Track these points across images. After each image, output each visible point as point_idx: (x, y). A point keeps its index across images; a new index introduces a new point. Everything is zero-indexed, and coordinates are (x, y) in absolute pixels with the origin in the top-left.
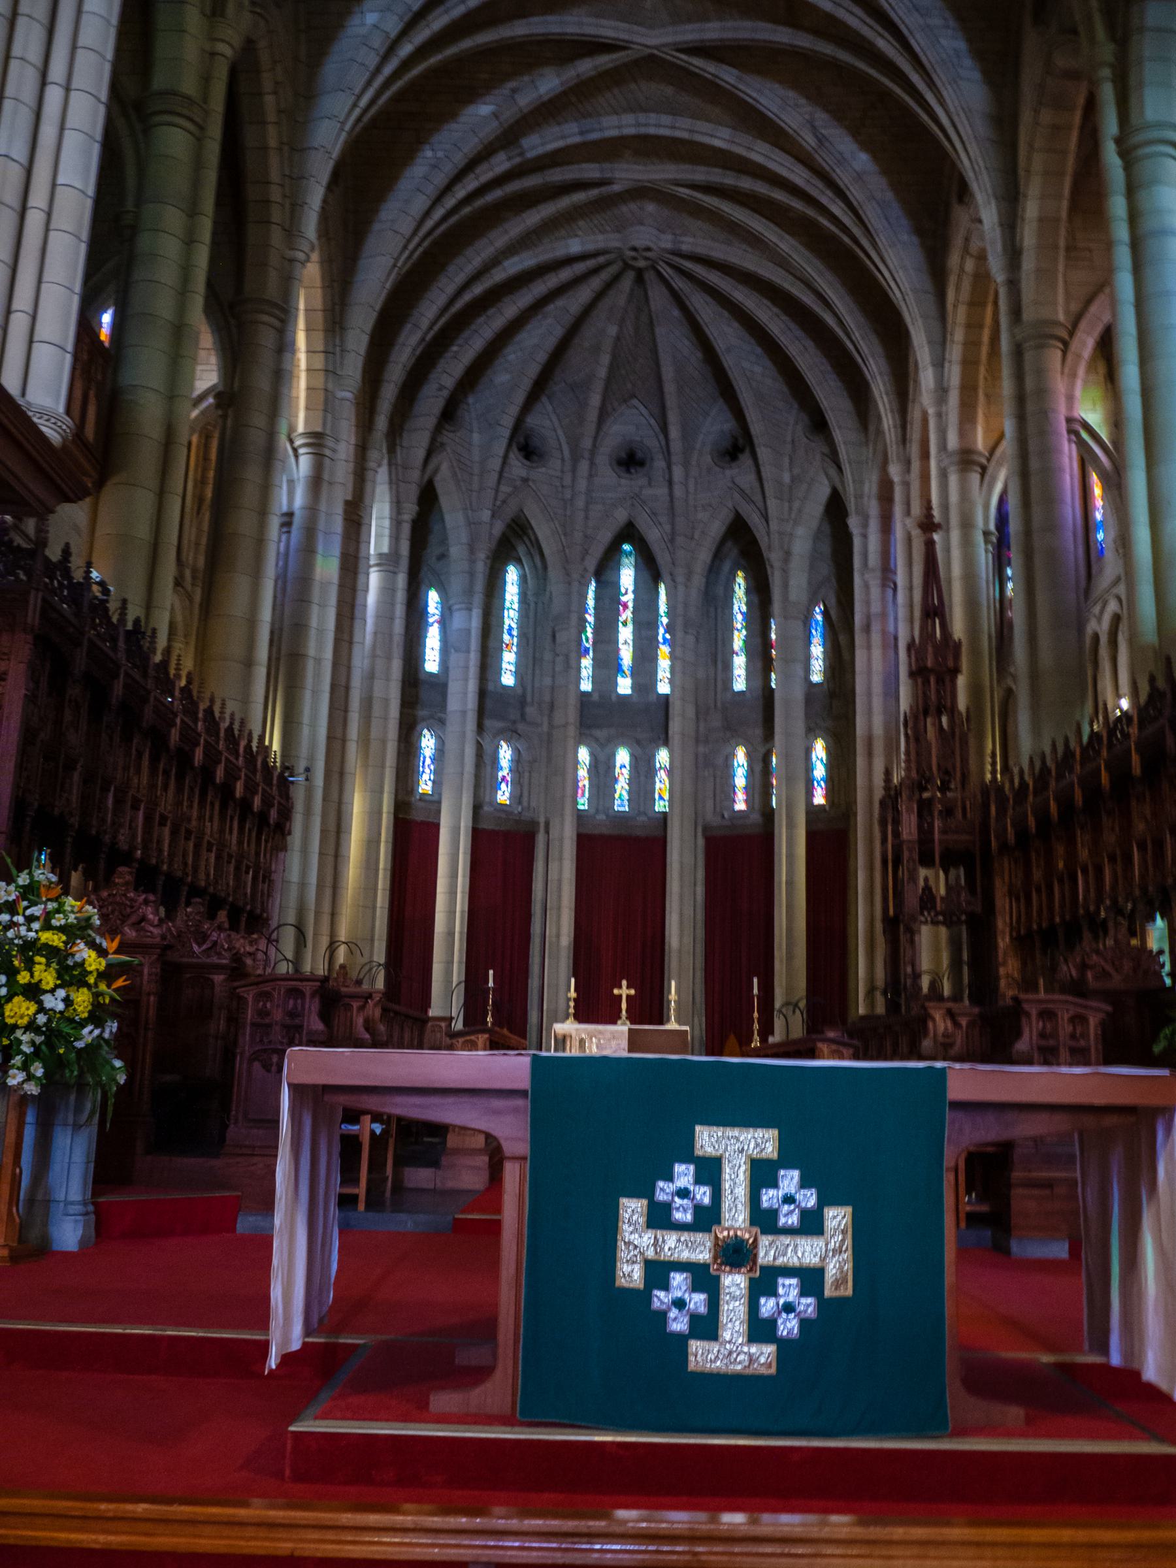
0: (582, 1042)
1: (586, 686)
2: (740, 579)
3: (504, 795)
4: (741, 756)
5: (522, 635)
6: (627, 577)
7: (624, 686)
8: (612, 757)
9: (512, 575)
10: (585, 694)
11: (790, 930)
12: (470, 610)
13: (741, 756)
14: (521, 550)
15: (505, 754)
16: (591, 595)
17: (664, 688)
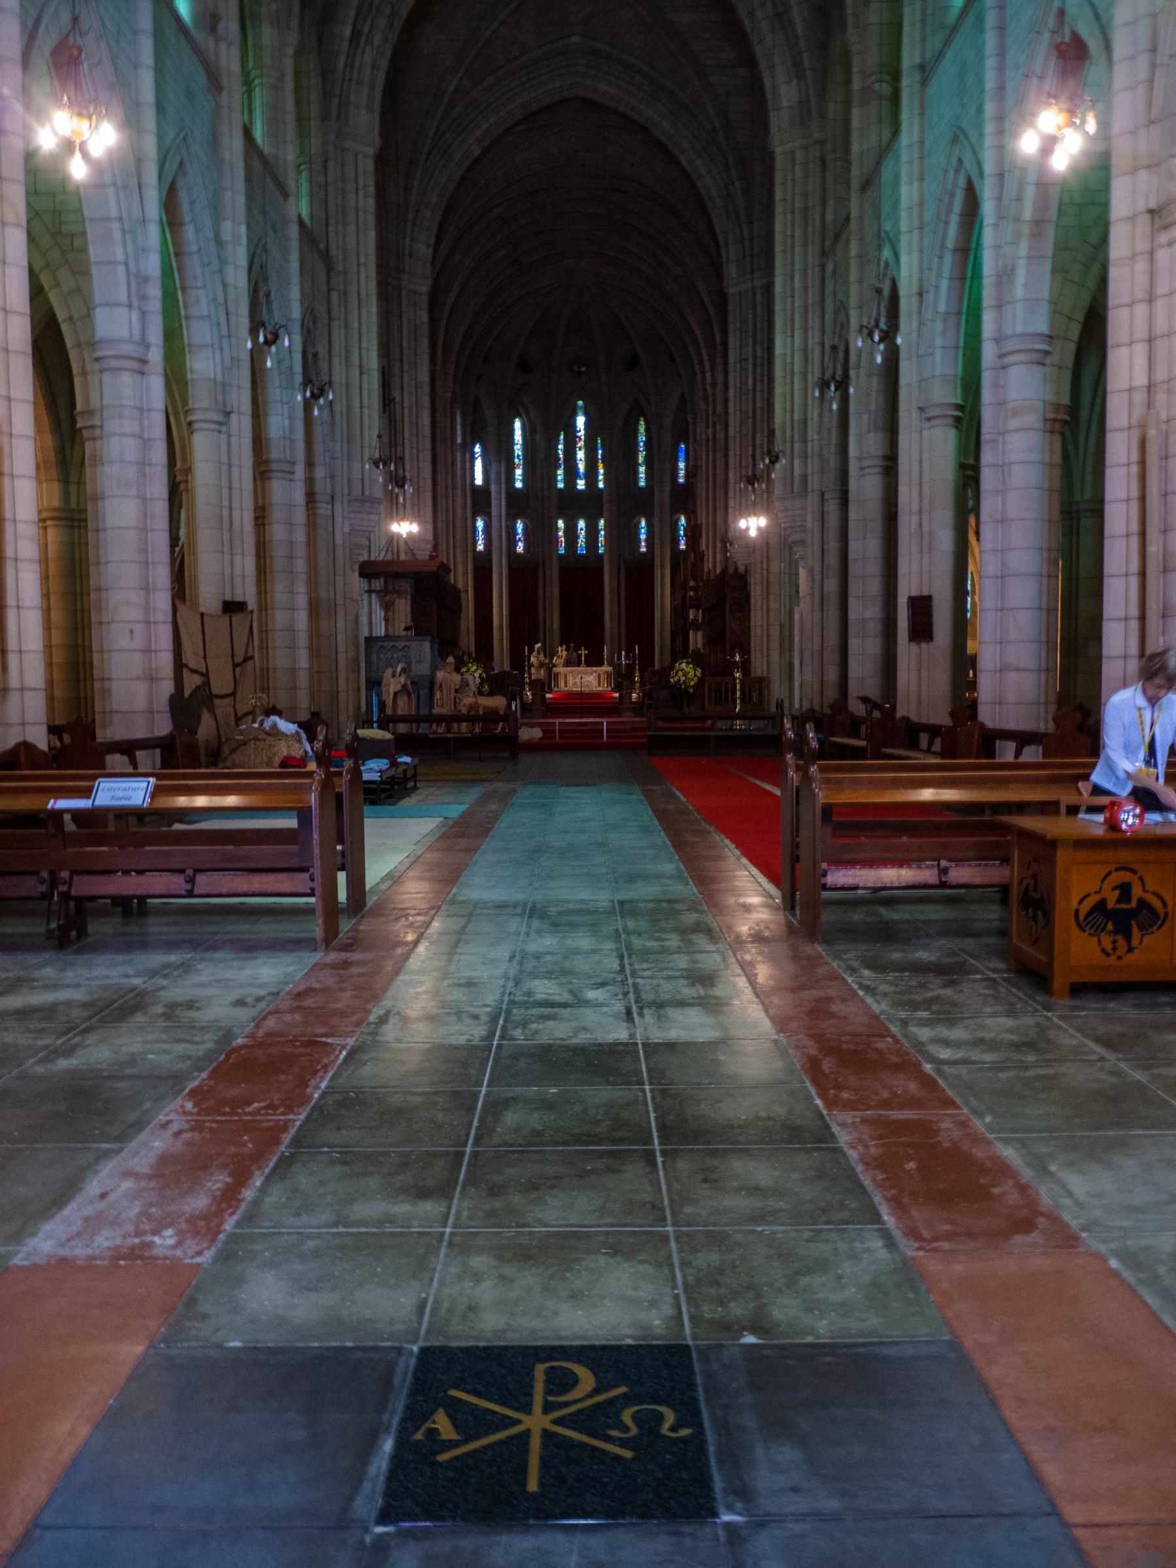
0: (565, 676)
1: (561, 485)
2: (642, 423)
3: (520, 547)
4: (643, 523)
5: (526, 459)
6: (581, 421)
7: (581, 484)
8: (576, 526)
9: (518, 424)
10: (560, 490)
11: (662, 618)
12: (500, 461)
13: (643, 523)
14: (521, 411)
15: (520, 526)
16: (562, 437)
17: (601, 485)
